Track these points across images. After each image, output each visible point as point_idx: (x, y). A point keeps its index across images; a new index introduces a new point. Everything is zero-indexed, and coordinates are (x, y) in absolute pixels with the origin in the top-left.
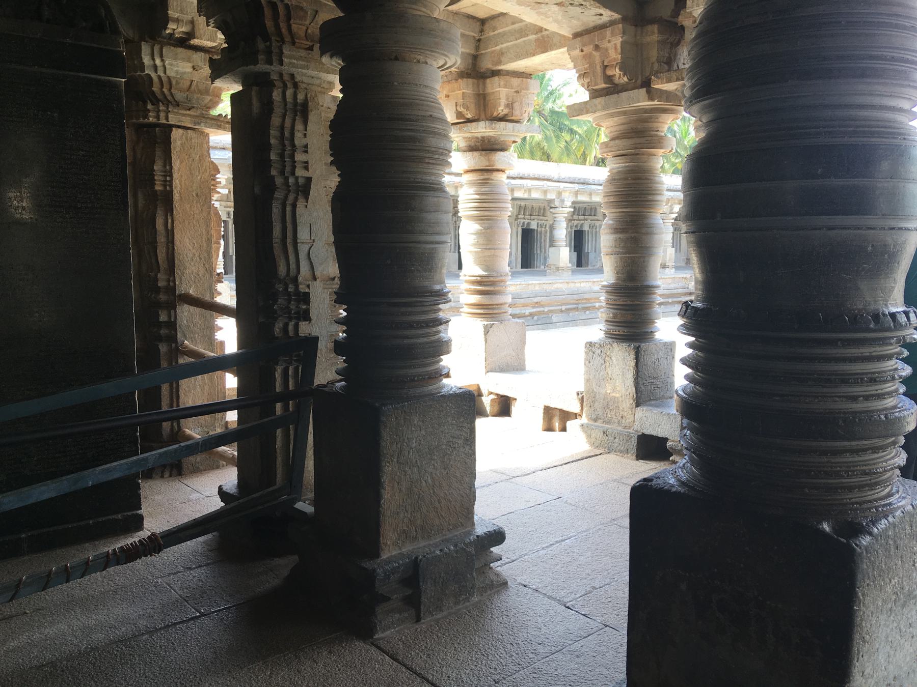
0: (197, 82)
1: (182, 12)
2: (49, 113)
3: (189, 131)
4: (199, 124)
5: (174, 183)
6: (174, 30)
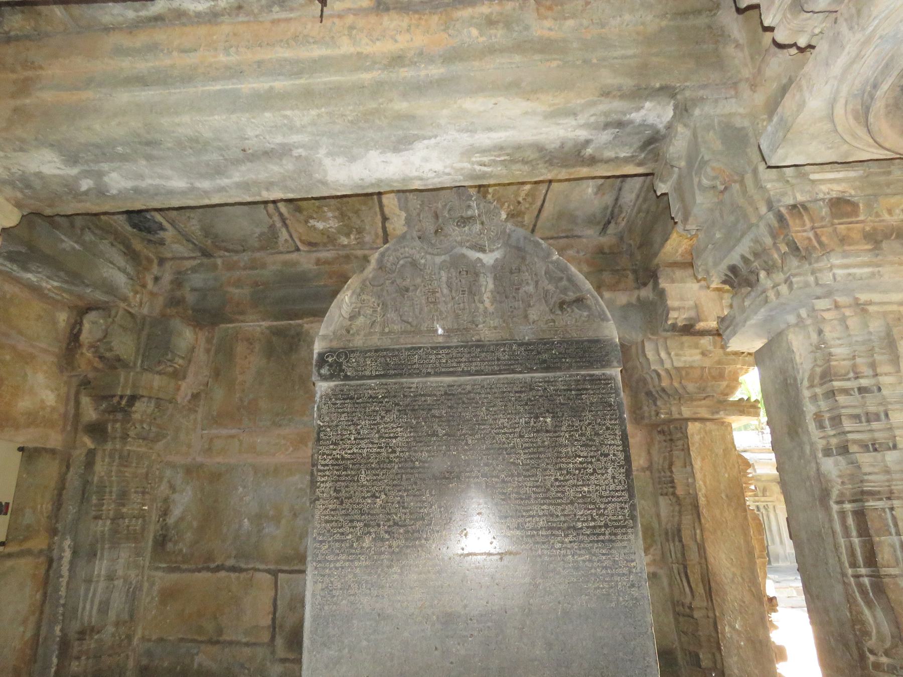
0: (709, 368)
1: (682, 299)
2: (542, 419)
3: (708, 424)
4: (717, 413)
5: (697, 485)
6: (676, 318)
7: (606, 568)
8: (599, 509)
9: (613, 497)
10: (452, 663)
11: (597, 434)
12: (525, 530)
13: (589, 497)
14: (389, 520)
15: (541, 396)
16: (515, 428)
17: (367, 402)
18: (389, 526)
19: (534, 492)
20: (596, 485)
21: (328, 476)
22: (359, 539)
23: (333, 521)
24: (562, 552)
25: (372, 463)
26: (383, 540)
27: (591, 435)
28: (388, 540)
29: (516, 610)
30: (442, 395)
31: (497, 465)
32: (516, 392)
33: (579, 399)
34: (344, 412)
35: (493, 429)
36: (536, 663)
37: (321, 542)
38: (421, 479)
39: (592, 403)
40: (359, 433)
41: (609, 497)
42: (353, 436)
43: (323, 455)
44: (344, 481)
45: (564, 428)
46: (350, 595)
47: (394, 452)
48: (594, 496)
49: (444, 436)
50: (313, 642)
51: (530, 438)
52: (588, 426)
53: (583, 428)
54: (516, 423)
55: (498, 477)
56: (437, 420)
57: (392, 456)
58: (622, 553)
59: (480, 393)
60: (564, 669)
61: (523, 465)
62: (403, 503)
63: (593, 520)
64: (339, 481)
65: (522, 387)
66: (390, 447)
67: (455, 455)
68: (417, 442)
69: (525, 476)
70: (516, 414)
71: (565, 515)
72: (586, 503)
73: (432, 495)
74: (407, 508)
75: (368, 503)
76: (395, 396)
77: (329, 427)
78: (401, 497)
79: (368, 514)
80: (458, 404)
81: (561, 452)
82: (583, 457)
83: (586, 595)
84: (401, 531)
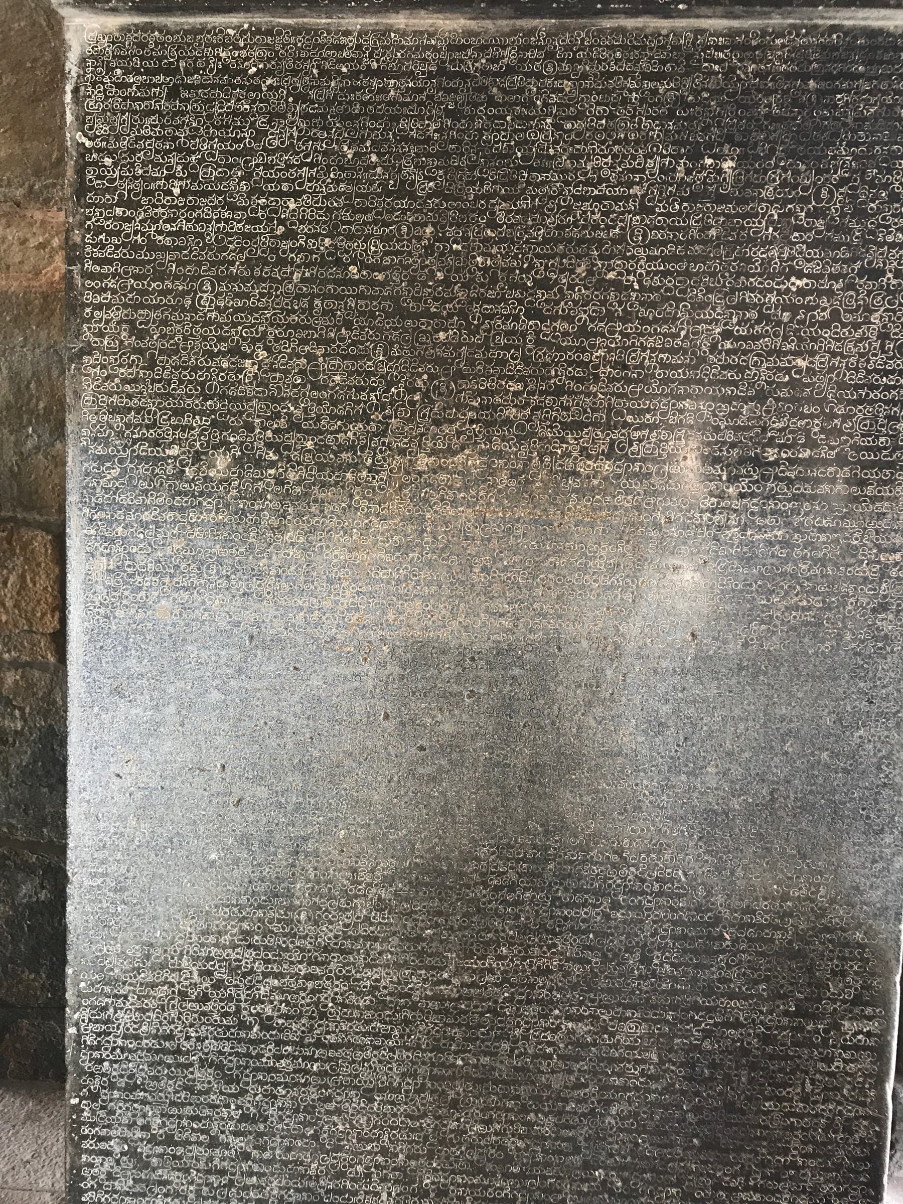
2: (709, 161)
7: (823, 562)
8: (833, 416)
9: (872, 387)
10: (422, 748)
11: (860, 214)
12: (628, 460)
13: (808, 385)
14: (278, 416)
15: (714, 93)
16: (630, 185)
17: (213, 87)
18: (276, 432)
19: (663, 365)
20: (834, 354)
21: (114, 292)
22: (197, 457)
23: (129, 410)
24: (716, 518)
25: (232, 263)
26: (259, 463)
27: (843, 215)
28: (272, 465)
29: (585, 644)
30: (431, 75)
31: (571, 287)
32: (646, 76)
33: (826, 106)
34: (150, 113)
35: (567, 183)
36: (620, 760)
37: (102, 459)
38: (362, 314)
39: (861, 120)
40: (194, 177)
41: (862, 387)
42: (176, 183)
43: (97, 234)
44: (156, 307)
45: (768, 192)
46: (178, 589)
47: (291, 234)
48: (822, 382)
49: (429, 196)
50: (92, 687)
51: (669, 215)
52: (838, 186)
53: (824, 194)
54: (634, 171)
55: (569, 319)
56: (414, 150)
57: (286, 245)
58: (871, 528)
59: (539, 76)
60: (683, 777)
61: (643, 289)
62: (315, 374)
63: (811, 444)
64: (142, 306)
65: (663, 62)
66: (281, 222)
67: (457, 253)
68: (356, 211)
69: (644, 321)
70: (637, 142)
71: (737, 429)
72: (798, 400)
73: (390, 359)
74: (325, 387)
75: (222, 370)
76: (295, 73)
77: (110, 154)
78: (310, 357)
79: (222, 397)
80: (476, 105)
81: (749, 261)
82: (809, 276)
83: (763, 622)
84: (309, 445)
